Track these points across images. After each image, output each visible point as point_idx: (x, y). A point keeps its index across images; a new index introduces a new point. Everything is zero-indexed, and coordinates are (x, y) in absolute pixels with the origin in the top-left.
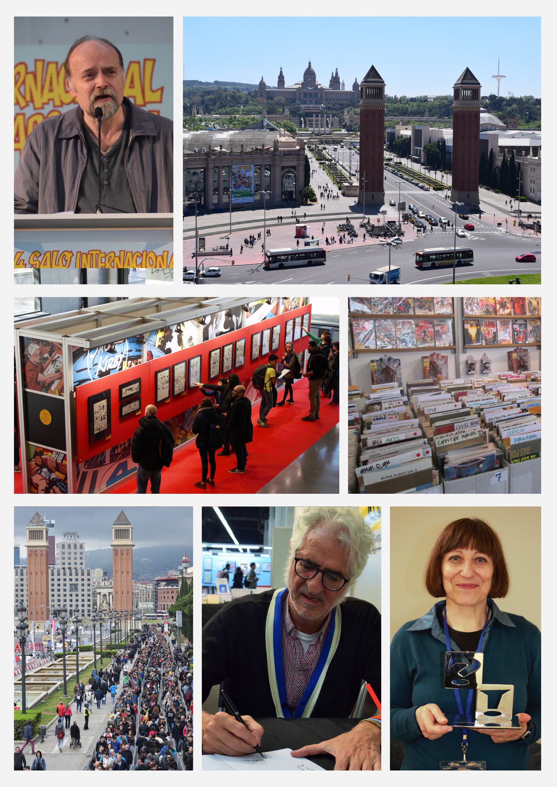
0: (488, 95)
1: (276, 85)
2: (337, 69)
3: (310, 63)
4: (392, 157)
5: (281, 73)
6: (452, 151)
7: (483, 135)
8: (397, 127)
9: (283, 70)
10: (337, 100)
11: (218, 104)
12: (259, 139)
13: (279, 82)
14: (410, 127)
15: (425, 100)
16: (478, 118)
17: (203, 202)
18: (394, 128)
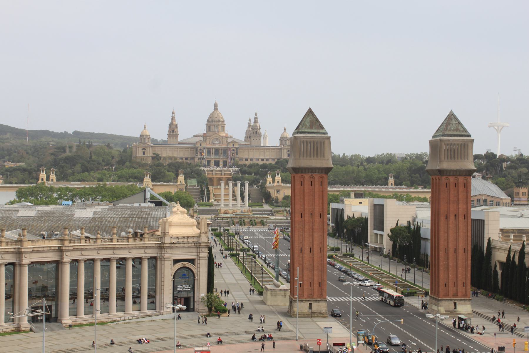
0: (483, 152)
1: (165, 138)
2: (256, 115)
3: (216, 106)
4: (340, 246)
5: (173, 118)
6: (429, 236)
7: (477, 212)
8: (347, 201)
9: (176, 115)
10: (257, 159)
11: (78, 168)
12: (139, 218)
13: (169, 132)
14: (366, 201)
15: (388, 160)
16: (467, 186)
17: (53, 313)
18: (343, 201)
